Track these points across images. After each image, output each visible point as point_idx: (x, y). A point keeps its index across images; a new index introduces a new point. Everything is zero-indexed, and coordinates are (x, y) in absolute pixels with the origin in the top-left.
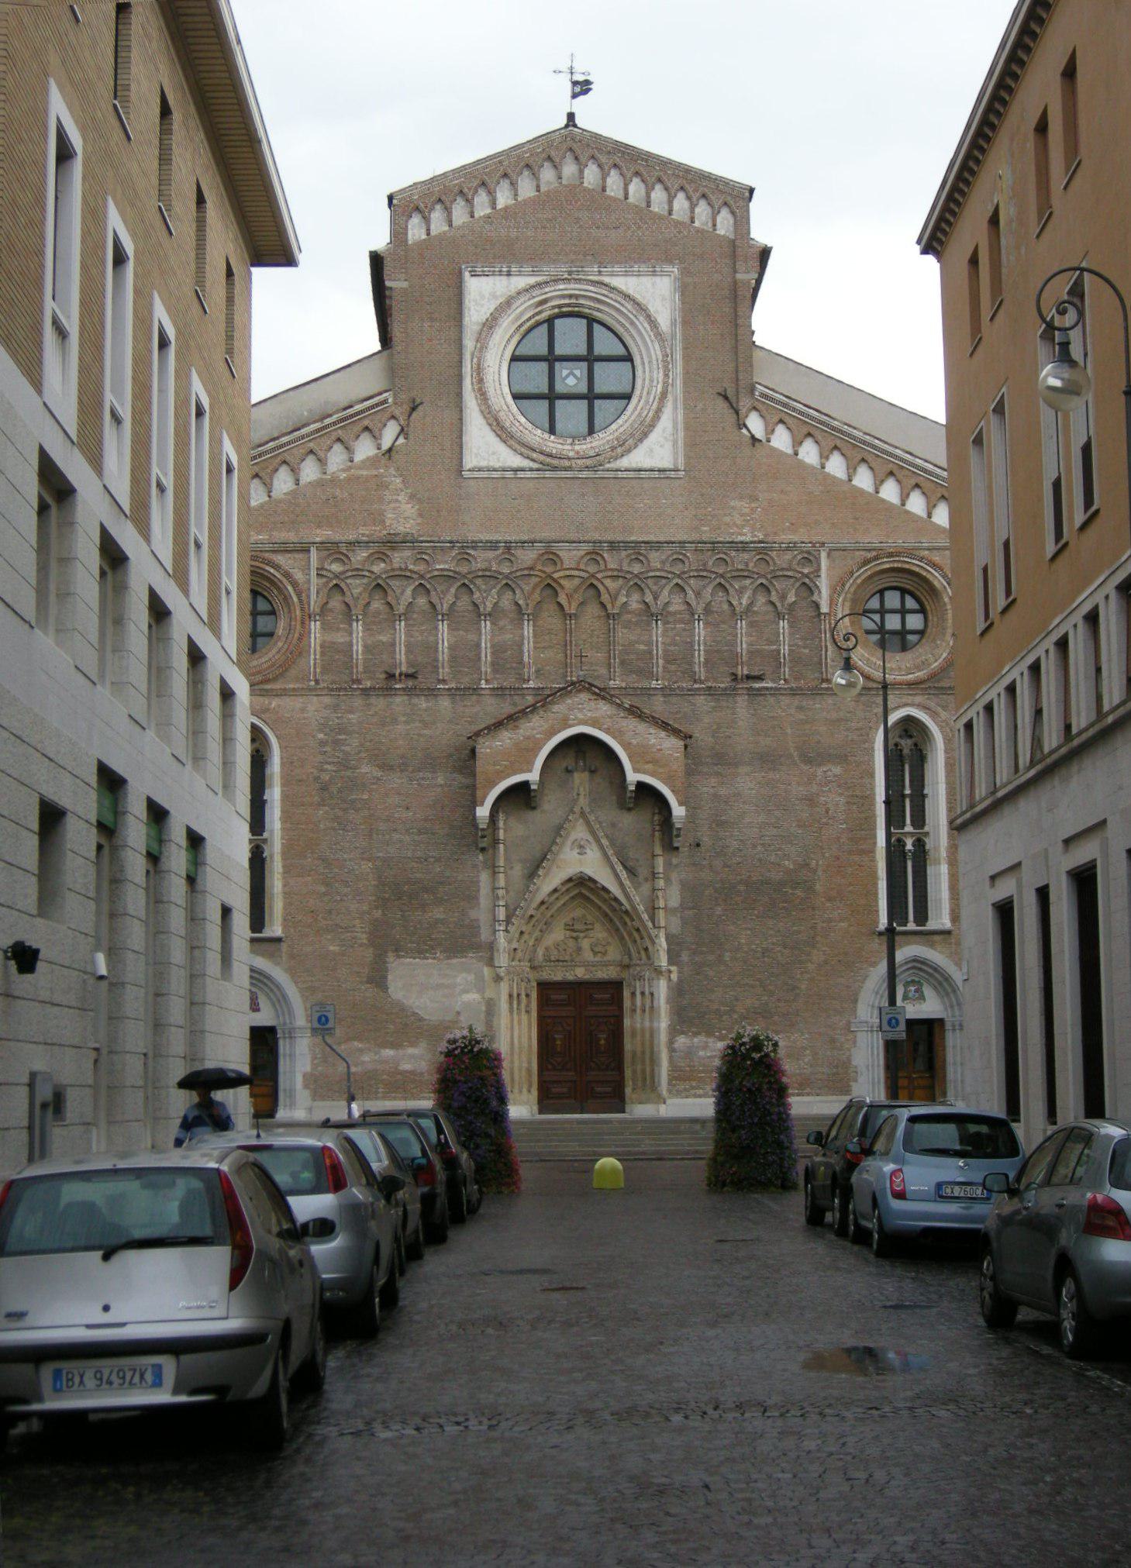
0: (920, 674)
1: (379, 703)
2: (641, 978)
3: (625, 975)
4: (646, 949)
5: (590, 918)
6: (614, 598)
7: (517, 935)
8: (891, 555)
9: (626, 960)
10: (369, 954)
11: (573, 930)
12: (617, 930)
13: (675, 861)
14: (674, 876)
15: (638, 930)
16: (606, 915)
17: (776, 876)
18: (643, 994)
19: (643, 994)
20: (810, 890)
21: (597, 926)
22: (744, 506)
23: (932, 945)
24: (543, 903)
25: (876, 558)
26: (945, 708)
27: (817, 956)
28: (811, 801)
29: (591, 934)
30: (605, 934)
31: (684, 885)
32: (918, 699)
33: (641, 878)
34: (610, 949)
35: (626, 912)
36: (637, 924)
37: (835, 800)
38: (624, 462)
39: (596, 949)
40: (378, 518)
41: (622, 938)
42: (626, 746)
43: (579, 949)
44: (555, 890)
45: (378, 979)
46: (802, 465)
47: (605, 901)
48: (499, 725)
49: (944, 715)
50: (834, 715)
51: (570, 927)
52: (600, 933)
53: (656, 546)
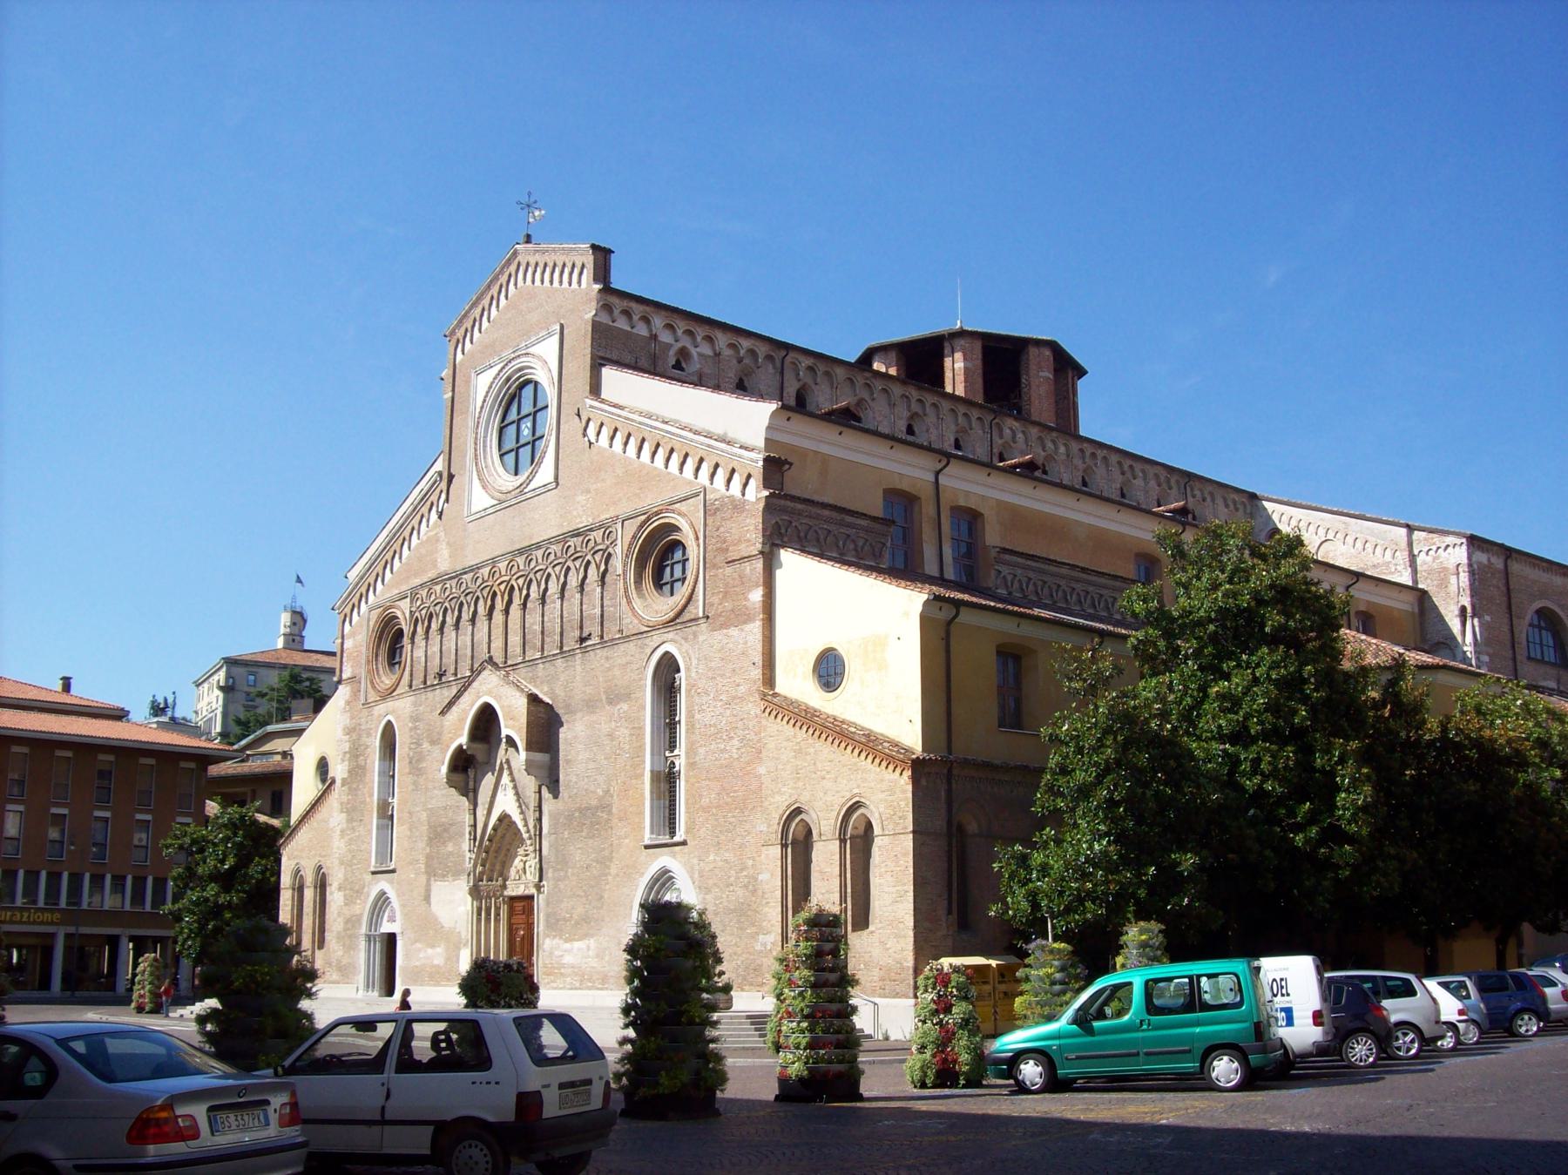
0: (672, 614)
1: (430, 695)
6: (520, 590)
8: (657, 513)
10: (423, 879)
17: (594, 803)
20: (610, 813)
22: (581, 498)
23: (674, 856)
25: (648, 519)
26: (686, 639)
27: (613, 871)
28: (611, 736)
32: (671, 636)
37: (624, 733)
38: (531, 487)
40: (434, 564)
42: (502, 707)
45: (427, 898)
46: (614, 455)
48: (451, 704)
49: (686, 646)
50: (624, 660)
53: (538, 546)
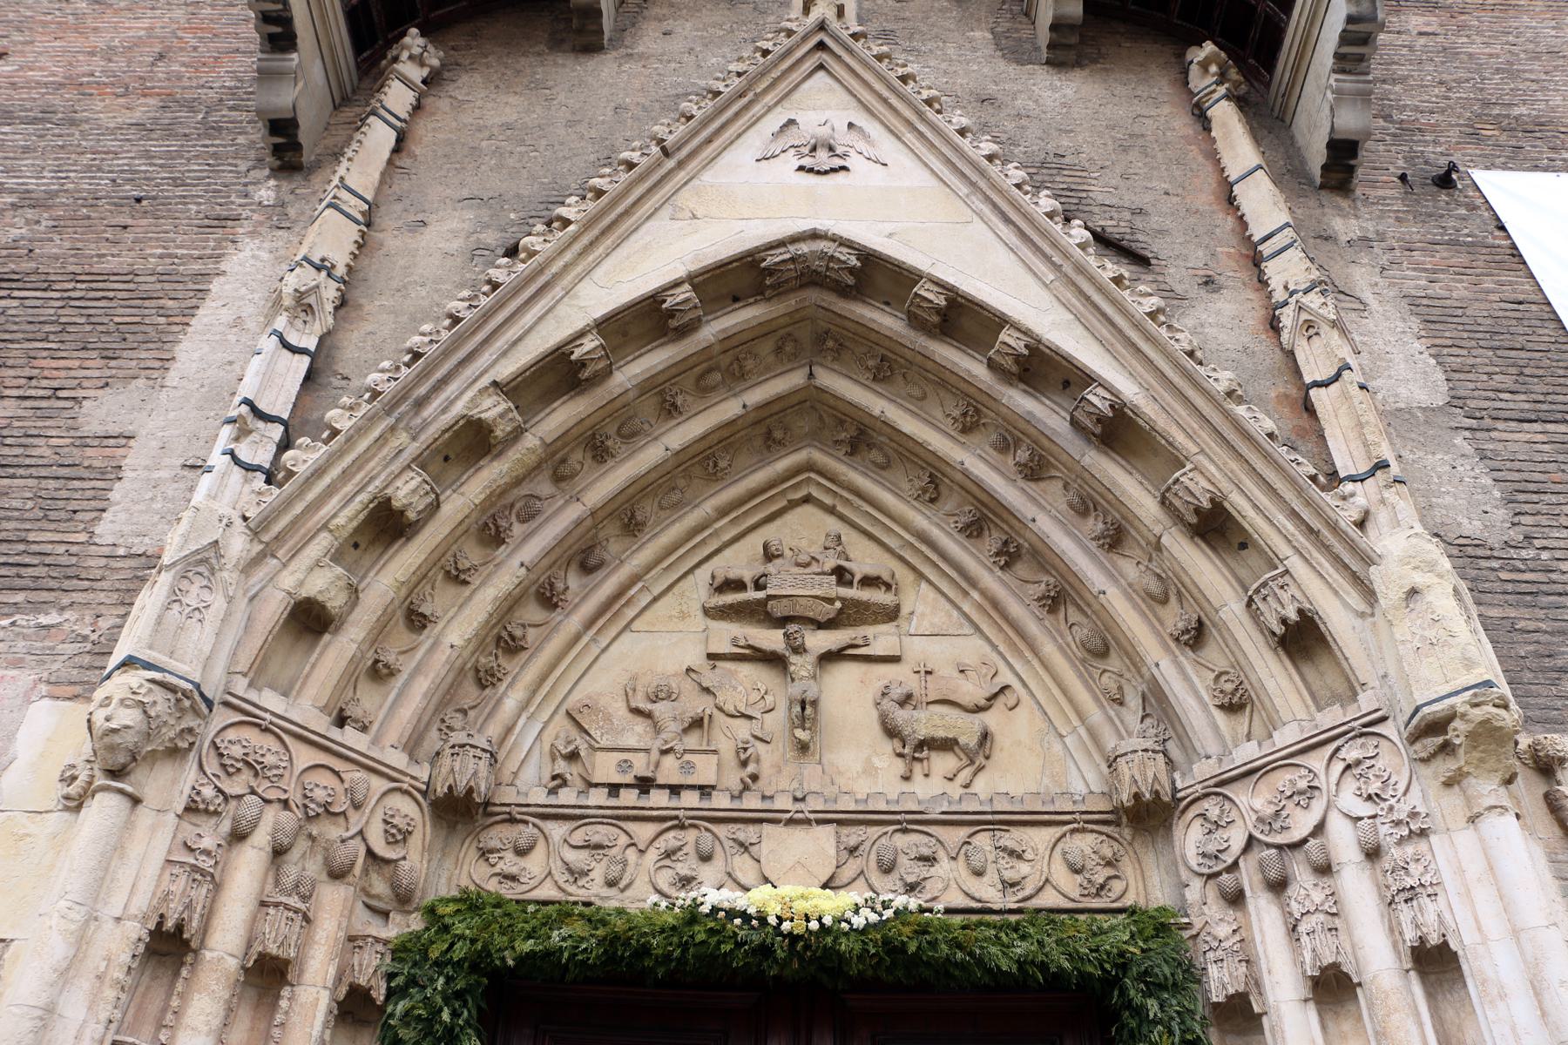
2: (1287, 861)
3: (1147, 884)
4: (1302, 639)
5: (865, 558)
7: (346, 513)
9: (1143, 774)
11: (758, 612)
12: (1060, 597)
13: (1345, 226)
14: (1362, 277)
15: (1215, 527)
16: (983, 517)
18: (1332, 988)
19: (1332, 988)
21: (923, 605)
24: (560, 373)
29: (881, 639)
30: (971, 649)
31: (1433, 318)
33: (1177, 276)
34: (1015, 729)
35: (1118, 431)
36: (1208, 473)
39: (926, 722)
41: (1102, 647)
43: (806, 710)
44: (647, 319)
47: (972, 416)
51: (741, 602)
52: (935, 638)
